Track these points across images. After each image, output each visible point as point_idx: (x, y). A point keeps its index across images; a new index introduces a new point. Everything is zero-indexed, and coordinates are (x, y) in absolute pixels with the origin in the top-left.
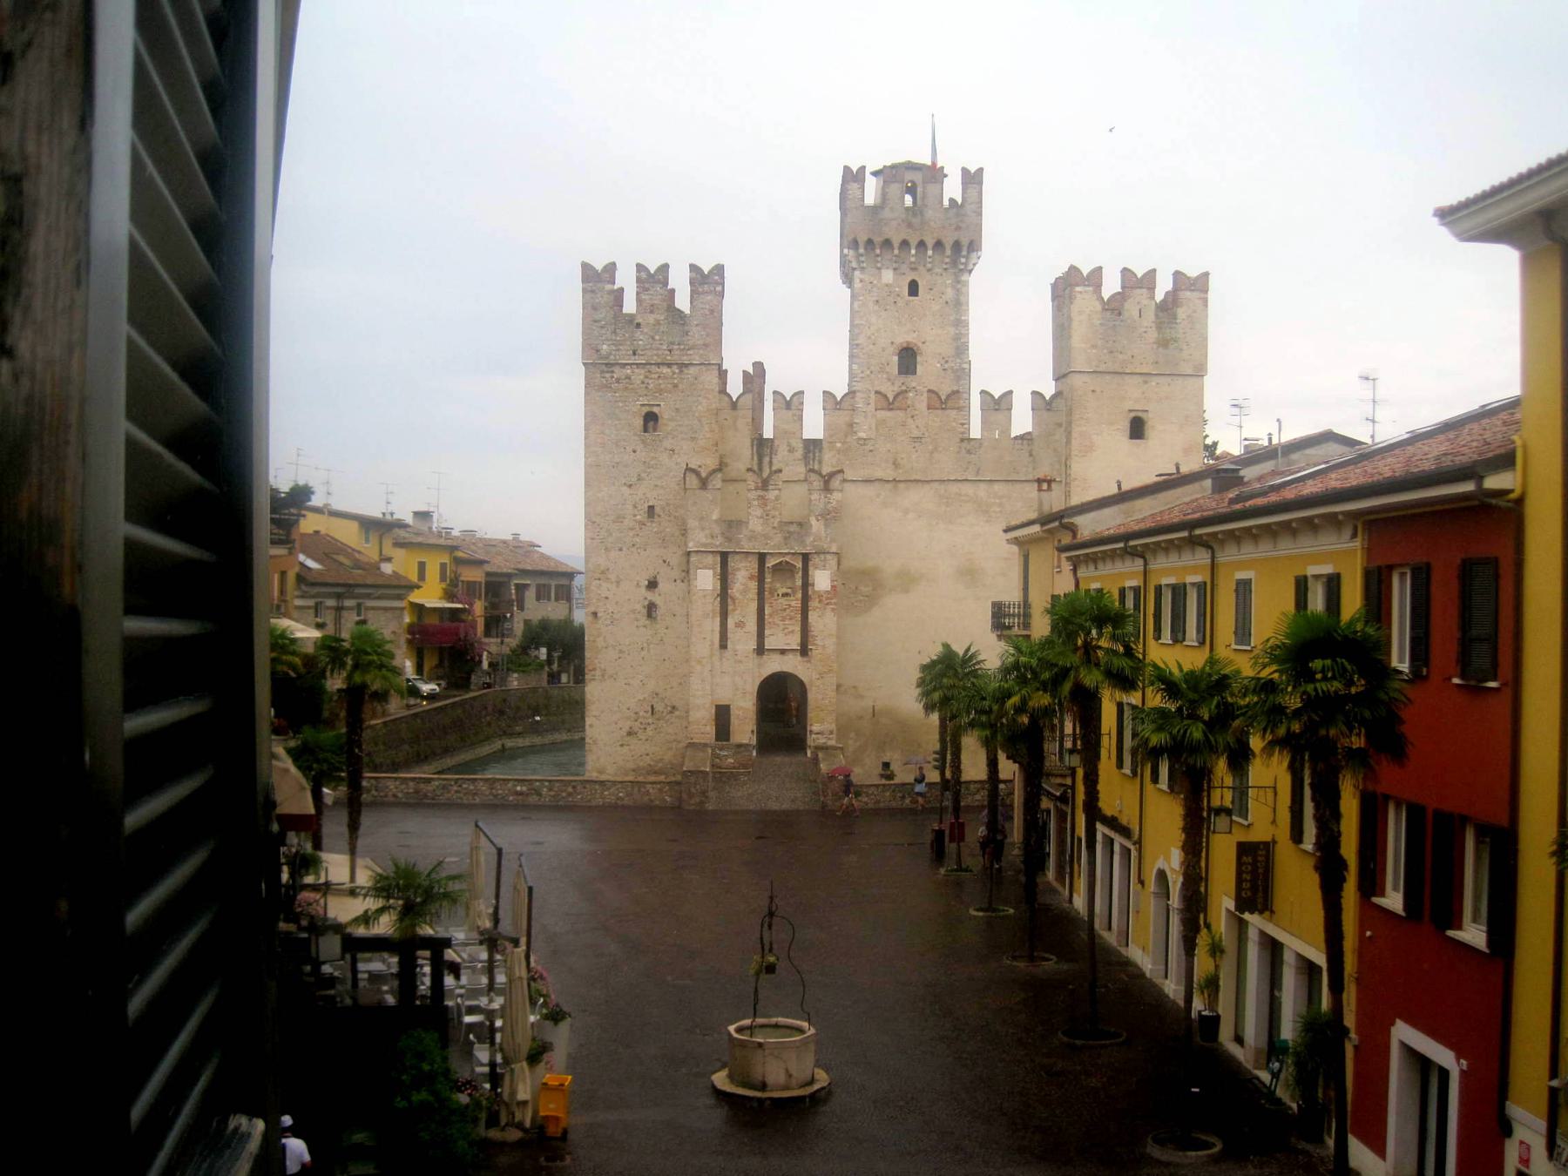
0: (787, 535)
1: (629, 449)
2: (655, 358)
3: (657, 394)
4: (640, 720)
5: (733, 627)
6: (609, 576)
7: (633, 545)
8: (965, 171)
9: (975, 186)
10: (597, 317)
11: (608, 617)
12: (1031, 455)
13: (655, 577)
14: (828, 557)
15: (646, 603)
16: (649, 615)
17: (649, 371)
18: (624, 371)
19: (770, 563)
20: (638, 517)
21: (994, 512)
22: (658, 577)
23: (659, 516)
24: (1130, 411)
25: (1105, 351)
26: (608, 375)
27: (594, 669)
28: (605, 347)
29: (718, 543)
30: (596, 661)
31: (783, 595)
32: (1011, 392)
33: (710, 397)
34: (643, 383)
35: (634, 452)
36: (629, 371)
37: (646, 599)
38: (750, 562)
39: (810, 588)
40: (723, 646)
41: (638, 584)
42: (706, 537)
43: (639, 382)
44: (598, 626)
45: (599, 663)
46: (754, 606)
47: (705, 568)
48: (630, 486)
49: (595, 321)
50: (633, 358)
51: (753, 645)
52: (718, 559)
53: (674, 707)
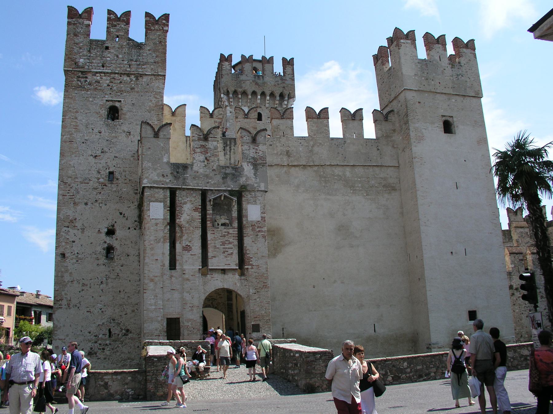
1: (96, 130)
2: (119, 69)
3: (119, 94)
4: (99, 342)
5: (181, 251)
6: (76, 225)
7: (96, 201)
8: (284, 60)
9: (290, 66)
10: (77, 41)
11: (74, 256)
12: (378, 149)
13: (113, 226)
14: (258, 194)
15: (106, 245)
17: (114, 78)
18: (95, 77)
19: (211, 197)
20: (101, 180)
23: (117, 179)
24: (443, 116)
25: (423, 78)
26: (82, 80)
27: (61, 300)
28: (82, 60)
29: (168, 181)
30: (63, 293)
31: (222, 225)
32: (361, 109)
34: (108, 85)
35: (100, 133)
36: (98, 78)
37: (105, 242)
39: (244, 219)
40: (173, 265)
41: (99, 231)
42: (158, 175)
43: (106, 85)
44: (65, 264)
45: (66, 294)
46: (198, 233)
47: (157, 201)
48: (96, 156)
50: (102, 68)
51: (198, 265)
52: (168, 193)
53: (128, 331)
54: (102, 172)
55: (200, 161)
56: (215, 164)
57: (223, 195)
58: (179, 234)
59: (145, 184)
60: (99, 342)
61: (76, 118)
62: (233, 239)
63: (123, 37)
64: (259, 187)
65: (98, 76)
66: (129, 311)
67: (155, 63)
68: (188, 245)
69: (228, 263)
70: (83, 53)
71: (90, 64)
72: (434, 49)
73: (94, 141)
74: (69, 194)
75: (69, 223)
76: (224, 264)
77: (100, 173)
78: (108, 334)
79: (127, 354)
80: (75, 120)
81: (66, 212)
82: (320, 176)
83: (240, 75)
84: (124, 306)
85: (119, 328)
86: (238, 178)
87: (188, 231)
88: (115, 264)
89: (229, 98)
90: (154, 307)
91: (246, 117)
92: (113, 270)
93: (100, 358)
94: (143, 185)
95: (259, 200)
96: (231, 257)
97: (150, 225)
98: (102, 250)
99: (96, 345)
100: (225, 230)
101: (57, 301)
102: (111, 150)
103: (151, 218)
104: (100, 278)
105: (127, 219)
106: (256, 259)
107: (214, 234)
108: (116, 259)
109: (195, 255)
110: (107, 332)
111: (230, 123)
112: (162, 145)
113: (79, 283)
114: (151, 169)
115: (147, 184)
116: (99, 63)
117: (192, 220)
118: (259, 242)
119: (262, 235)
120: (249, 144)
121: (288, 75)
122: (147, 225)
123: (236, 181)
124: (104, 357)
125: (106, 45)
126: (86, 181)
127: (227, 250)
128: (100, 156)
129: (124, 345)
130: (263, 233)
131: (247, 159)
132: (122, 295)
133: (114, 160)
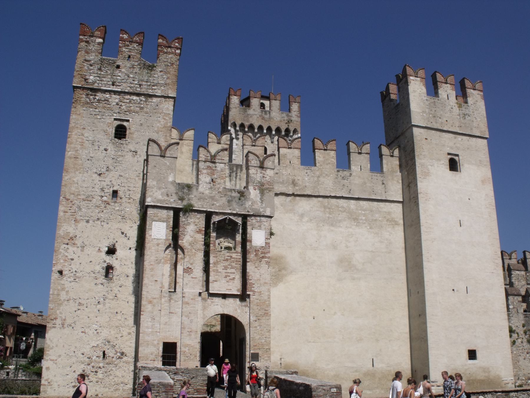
0: (230, 199)
1: (102, 148)
2: (129, 88)
3: (127, 113)
4: (93, 364)
5: (182, 273)
6: (76, 242)
7: (98, 219)
9: (296, 103)
10: (87, 58)
11: (72, 274)
12: (383, 184)
13: (114, 245)
16: (107, 275)
20: (105, 198)
21: (362, 219)
22: (116, 245)
23: (121, 198)
26: (91, 97)
27: (56, 319)
28: (92, 77)
29: (172, 200)
30: (58, 312)
33: (167, 118)
36: (107, 96)
37: (105, 262)
38: (199, 219)
39: (248, 244)
41: (99, 249)
42: (162, 194)
43: (115, 104)
44: (62, 282)
45: (61, 313)
46: (200, 255)
47: (160, 220)
49: (86, 60)
50: (112, 87)
51: (199, 288)
52: (171, 213)
53: (122, 354)
54: (106, 191)
55: (206, 183)
56: (221, 186)
57: (228, 218)
58: (181, 256)
59: (149, 202)
60: (93, 364)
61: (83, 135)
62: (236, 264)
63: (135, 57)
64: (265, 212)
65: (107, 94)
66: (125, 333)
67: (166, 84)
68: (190, 267)
69: (229, 288)
70: (93, 71)
71: (101, 82)
72: (443, 88)
73: (99, 159)
74: (70, 211)
75: (69, 240)
76: (225, 289)
77: (104, 191)
78: (102, 356)
79: (120, 378)
80: (81, 137)
81: (66, 228)
82: (325, 207)
83: (247, 110)
84: (120, 328)
85: (114, 351)
86: (244, 202)
87: (189, 253)
88: (114, 285)
89: (236, 131)
90: (150, 330)
91: (254, 144)
92: (111, 291)
93: (92, 381)
94: (146, 204)
95: (264, 225)
96: (233, 283)
97: (151, 245)
98: (101, 270)
99: (89, 367)
100: (228, 254)
101: (51, 320)
102: (116, 168)
103: (152, 237)
104: (97, 298)
105: (129, 239)
106: (259, 285)
107: (217, 257)
108: (115, 280)
109: (196, 278)
110: (101, 354)
111: (236, 155)
112: (168, 164)
113: (76, 302)
114: (155, 188)
115: (150, 202)
116: (109, 82)
117: (195, 241)
118: (262, 268)
119: (265, 261)
120: (257, 168)
121: (294, 111)
122: (149, 244)
123: (242, 205)
124: (96, 380)
125: (117, 64)
126: (88, 199)
127: (229, 274)
128: (105, 174)
129: (118, 369)
130: (266, 260)
131: (254, 183)
132: (119, 317)
133: (118, 179)
